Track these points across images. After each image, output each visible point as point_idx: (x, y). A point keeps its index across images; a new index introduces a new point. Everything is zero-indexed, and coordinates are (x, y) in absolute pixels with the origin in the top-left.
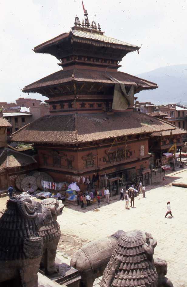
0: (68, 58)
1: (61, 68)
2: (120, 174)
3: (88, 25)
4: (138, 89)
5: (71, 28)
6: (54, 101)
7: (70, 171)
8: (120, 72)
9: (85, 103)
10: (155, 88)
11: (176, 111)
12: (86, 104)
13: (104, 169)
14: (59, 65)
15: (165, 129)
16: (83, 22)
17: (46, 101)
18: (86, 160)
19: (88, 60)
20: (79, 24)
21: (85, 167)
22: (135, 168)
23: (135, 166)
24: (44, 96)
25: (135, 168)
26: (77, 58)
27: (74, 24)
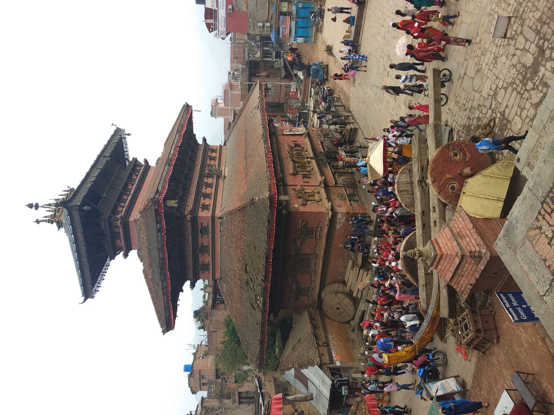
0: (115, 236)
1: (133, 253)
5: (59, 229)
6: (192, 268)
7: (326, 230)
8: (156, 164)
13: (322, 174)
14: (126, 255)
16: (50, 211)
17: (193, 286)
18: (308, 201)
21: (320, 203)
22: (323, 143)
23: (319, 142)
24: (183, 288)
25: (322, 143)
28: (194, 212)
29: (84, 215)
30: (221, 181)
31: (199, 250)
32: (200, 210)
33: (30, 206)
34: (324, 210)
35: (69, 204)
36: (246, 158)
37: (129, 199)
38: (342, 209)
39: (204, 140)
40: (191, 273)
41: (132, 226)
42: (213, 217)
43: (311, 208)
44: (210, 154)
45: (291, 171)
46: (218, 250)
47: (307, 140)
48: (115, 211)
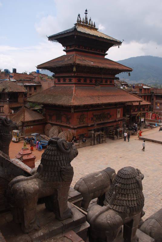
0: (70, 46)
1: (65, 53)
2: (102, 130)
3: (87, 22)
4: (119, 71)
5: (75, 24)
7: (68, 126)
8: (106, 58)
9: (81, 79)
10: (131, 71)
11: (143, 88)
12: (81, 80)
14: (64, 50)
15: (134, 99)
19: (84, 49)
20: (80, 22)
26: (77, 47)
27: (77, 21)
29: (73, 36)
30: (94, 86)
31: (64, 78)
32: (78, 79)
33: (86, 11)
36: (99, 96)
40: (57, 75)
44: (108, 80)
45: (94, 114)
46: (65, 86)
47: (113, 120)
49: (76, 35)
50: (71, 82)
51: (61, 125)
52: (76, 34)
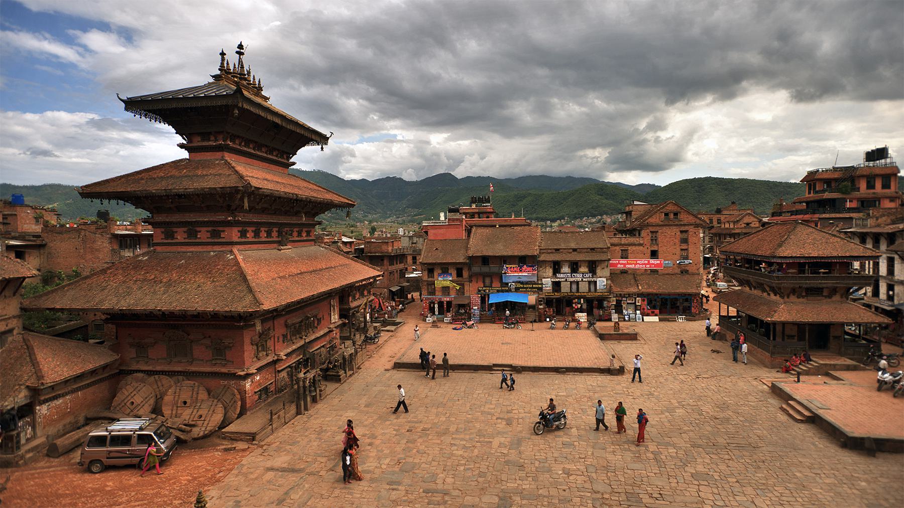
0: (205, 136)
1: (184, 154)
5: (213, 77)
7: (224, 370)
13: (287, 355)
14: (181, 146)
21: (255, 359)
25: (323, 346)
28: (236, 223)
30: (275, 245)
31: (192, 229)
32: (240, 229)
34: (247, 364)
35: (239, 96)
36: (301, 273)
37: (249, 150)
38: (248, 385)
39: (320, 223)
41: (218, 155)
42: (232, 243)
43: (249, 351)
47: (326, 330)
48: (233, 138)
49: (239, 108)
50: (221, 238)
51: (193, 372)
52: (240, 105)
